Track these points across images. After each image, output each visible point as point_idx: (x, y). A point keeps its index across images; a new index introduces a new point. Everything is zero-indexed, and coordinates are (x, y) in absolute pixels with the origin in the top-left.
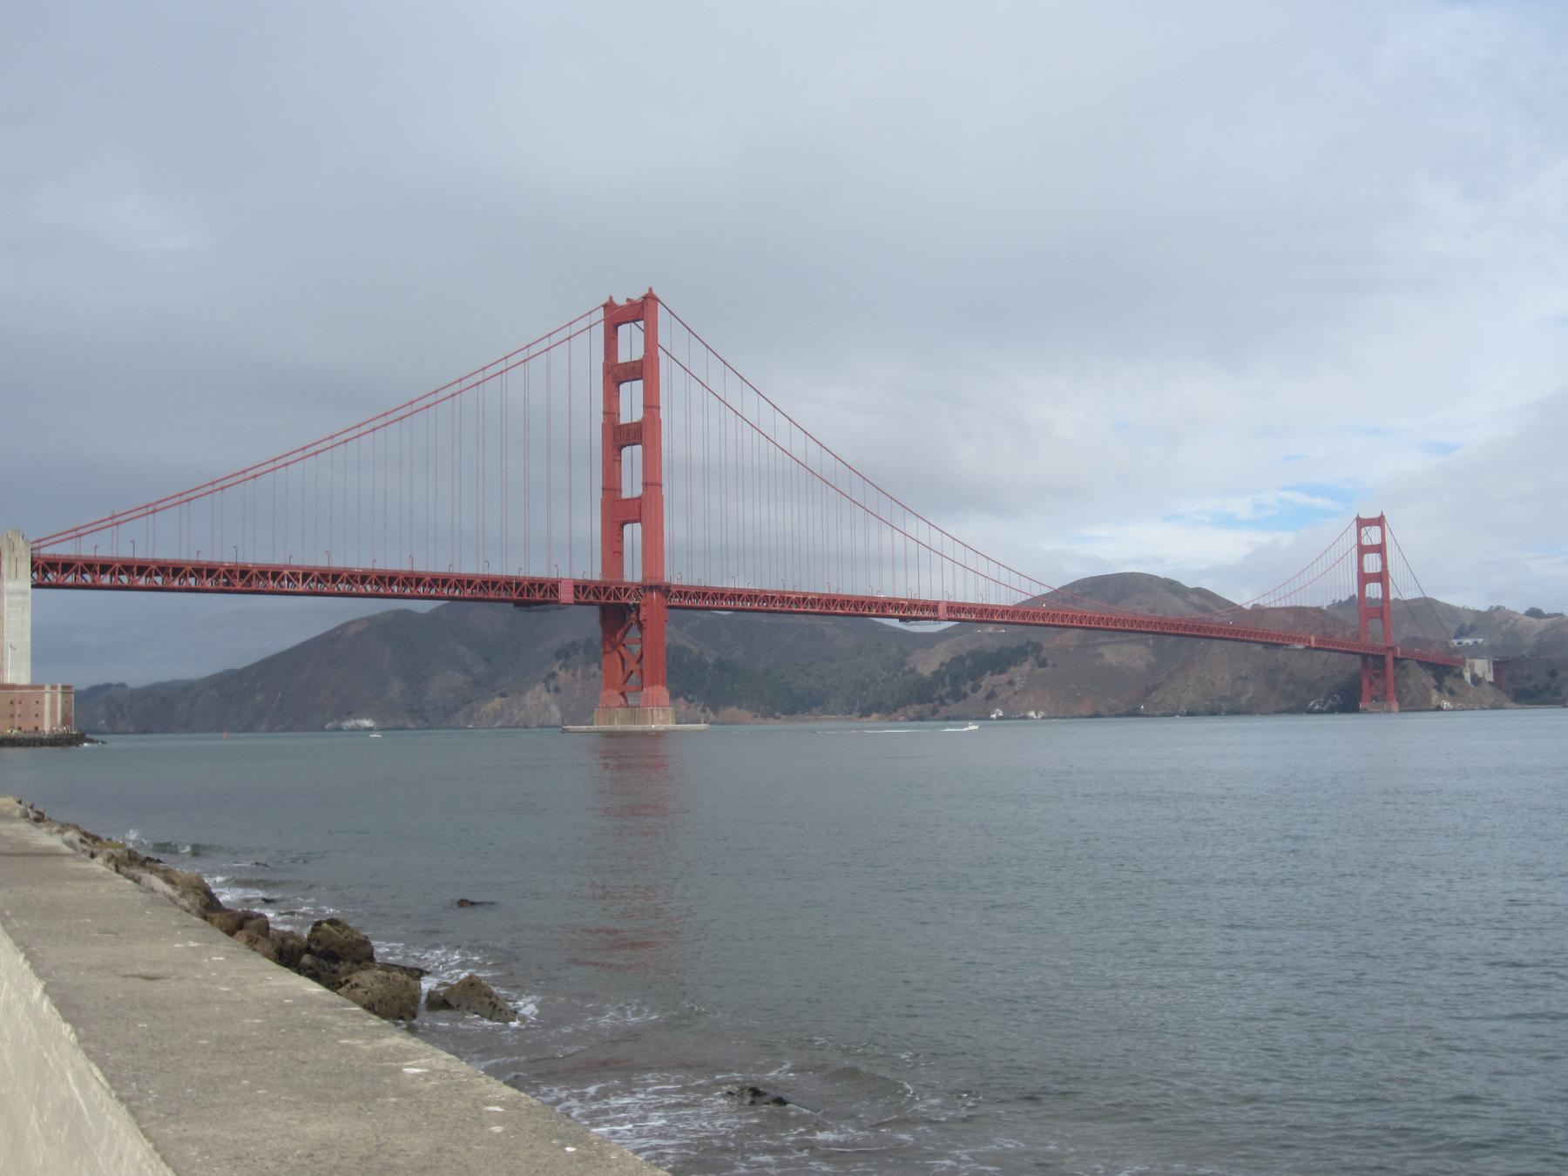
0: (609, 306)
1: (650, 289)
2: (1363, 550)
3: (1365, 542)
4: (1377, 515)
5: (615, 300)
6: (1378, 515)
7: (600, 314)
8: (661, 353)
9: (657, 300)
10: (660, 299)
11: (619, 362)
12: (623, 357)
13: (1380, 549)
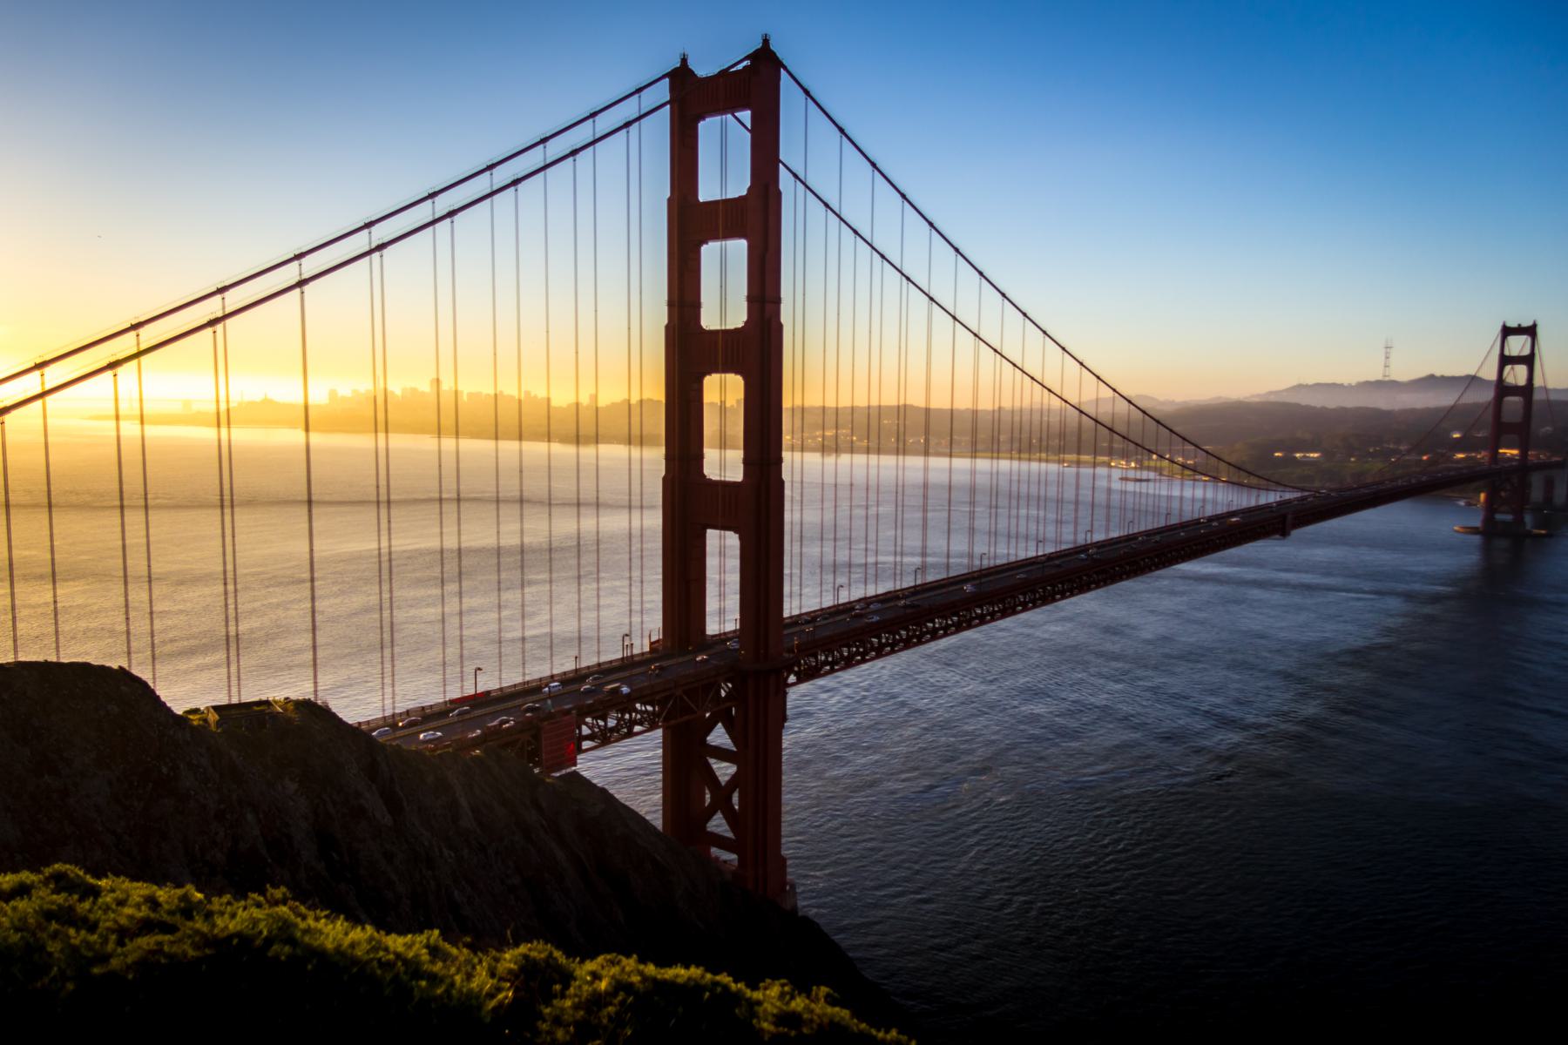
0: (681, 77)
1: (766, 41)
2: (1505, 360)
4: (1527, 323)
5: (692, 65)
6: (1530, 323)
7: (662, 92)
8: (785, 181)
9: (779, 64)
10: (785, 62)
11: (701, 199)
12: (708, 191)
13: (1529, 360)
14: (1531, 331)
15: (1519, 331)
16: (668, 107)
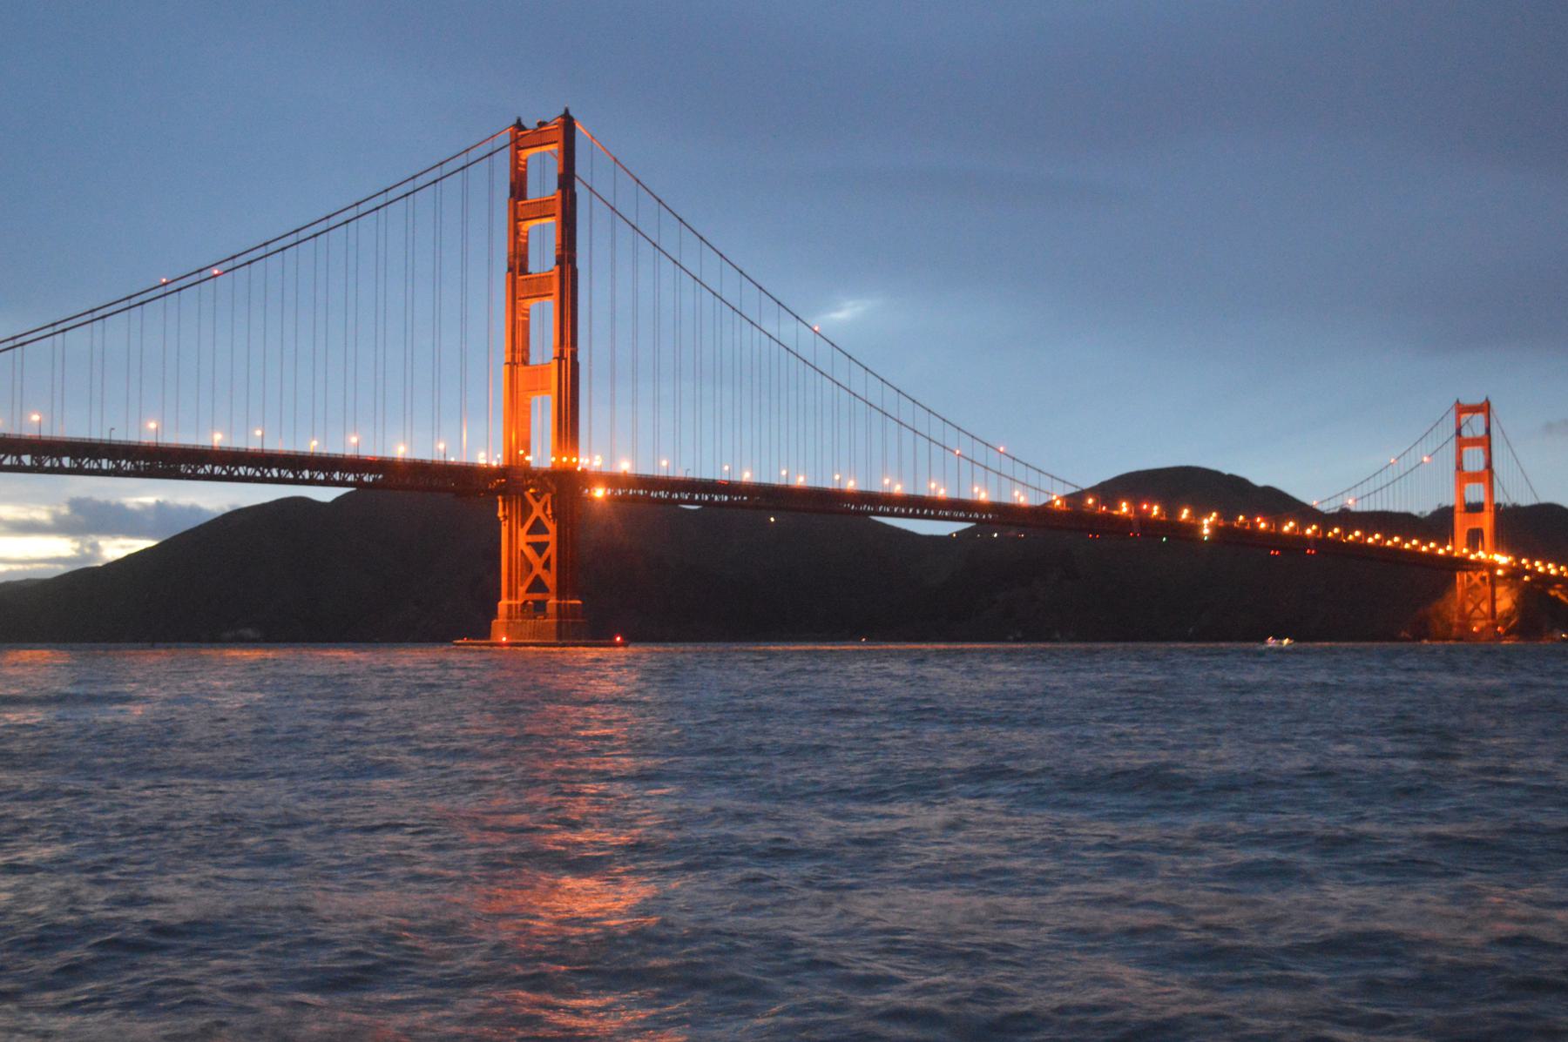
1: (567, 111)
3: (1466, 433)
5: (524, 123)
8: (579, 188)
12: (533, 193)
13: (1486, 442)
14: (1485, 408)
15: (1474, 409)
16: (508, 148)
